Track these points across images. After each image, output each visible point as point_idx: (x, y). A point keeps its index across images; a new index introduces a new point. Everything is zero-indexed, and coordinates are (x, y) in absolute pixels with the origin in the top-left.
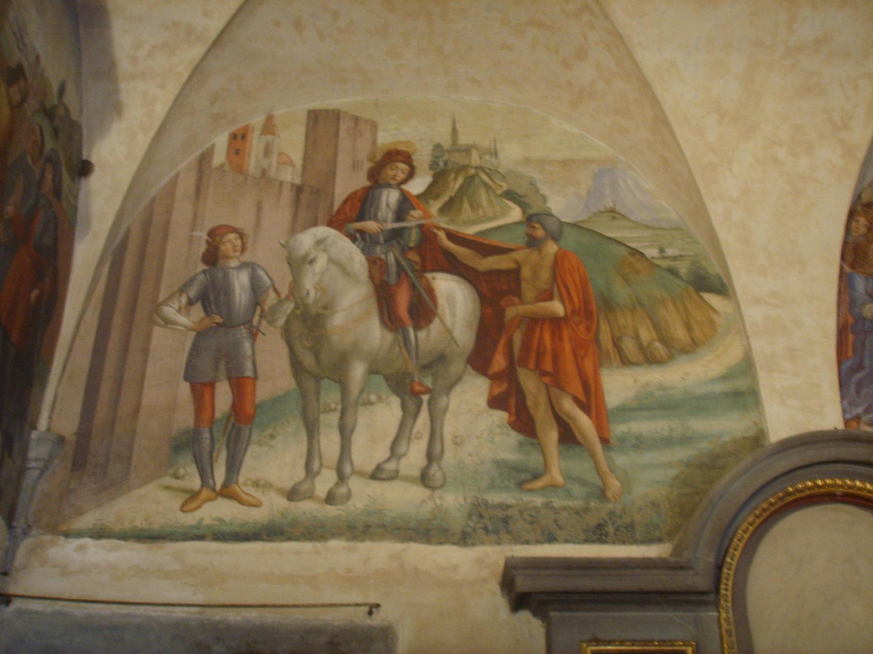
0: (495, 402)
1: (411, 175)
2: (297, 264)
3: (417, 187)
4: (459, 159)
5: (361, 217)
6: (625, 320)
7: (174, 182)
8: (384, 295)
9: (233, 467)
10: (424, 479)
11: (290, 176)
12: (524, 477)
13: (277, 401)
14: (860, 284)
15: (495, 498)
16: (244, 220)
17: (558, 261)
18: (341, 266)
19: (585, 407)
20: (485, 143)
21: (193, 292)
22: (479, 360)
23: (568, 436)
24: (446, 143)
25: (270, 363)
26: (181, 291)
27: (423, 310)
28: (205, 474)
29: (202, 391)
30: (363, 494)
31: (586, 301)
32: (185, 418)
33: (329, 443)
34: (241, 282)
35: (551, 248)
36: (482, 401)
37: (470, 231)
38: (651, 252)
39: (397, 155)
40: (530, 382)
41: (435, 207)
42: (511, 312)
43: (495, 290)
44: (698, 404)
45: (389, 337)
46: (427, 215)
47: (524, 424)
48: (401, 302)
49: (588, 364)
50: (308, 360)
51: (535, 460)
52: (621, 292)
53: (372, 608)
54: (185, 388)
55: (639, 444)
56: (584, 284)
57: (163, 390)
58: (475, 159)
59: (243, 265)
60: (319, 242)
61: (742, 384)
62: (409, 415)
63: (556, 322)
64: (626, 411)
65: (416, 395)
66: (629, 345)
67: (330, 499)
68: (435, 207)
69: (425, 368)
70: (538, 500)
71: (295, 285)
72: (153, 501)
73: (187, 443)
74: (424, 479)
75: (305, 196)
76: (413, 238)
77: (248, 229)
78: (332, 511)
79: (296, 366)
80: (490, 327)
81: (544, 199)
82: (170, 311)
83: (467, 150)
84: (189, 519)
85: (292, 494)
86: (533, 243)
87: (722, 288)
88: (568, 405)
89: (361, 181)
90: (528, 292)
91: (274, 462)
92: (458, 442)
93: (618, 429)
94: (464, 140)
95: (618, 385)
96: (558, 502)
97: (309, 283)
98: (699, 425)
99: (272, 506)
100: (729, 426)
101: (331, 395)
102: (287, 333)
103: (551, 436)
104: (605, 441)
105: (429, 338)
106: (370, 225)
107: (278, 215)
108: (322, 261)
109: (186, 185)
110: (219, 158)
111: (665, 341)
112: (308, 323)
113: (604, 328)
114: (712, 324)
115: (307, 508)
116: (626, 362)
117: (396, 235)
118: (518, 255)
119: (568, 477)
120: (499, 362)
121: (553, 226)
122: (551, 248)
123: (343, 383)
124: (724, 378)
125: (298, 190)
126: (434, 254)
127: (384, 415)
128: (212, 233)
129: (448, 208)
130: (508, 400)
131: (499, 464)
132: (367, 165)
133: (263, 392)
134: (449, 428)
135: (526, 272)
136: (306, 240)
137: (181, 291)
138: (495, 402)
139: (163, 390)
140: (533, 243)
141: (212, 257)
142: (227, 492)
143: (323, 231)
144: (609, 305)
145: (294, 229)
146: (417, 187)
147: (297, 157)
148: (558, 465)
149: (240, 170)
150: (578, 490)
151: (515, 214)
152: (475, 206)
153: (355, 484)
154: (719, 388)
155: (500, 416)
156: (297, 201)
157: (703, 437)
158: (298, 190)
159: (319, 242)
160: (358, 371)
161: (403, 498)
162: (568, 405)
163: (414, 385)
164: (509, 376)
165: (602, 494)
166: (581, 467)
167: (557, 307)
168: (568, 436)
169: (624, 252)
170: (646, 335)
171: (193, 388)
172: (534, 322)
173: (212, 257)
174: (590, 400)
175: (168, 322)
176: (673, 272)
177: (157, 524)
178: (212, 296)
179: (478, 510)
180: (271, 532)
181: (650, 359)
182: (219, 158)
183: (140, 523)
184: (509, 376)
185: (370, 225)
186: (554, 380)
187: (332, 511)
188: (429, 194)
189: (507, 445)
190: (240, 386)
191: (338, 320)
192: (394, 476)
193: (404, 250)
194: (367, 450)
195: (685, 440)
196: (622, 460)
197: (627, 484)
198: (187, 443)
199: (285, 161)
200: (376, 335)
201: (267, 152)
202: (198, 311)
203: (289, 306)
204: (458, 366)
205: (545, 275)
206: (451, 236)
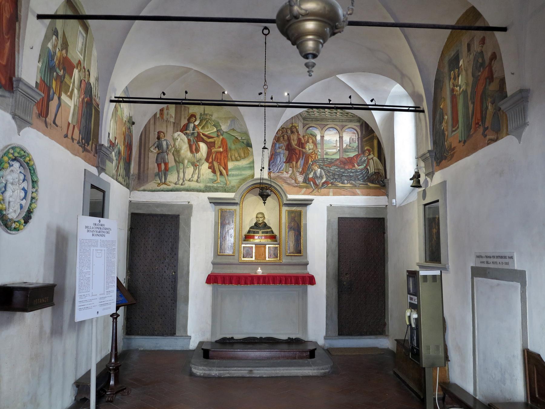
0: (209, 168)
1: (196, 120)
2: (175, 140)
3: (197, 123)
4: (205, 117)
5: (186, 130)
6: (233, 152)
7: (150, 120)
8: (190, 146)
9: (165, 179)
10: (197, 181)
11: (172, 120)
12: (214, 181)
13: (172, 167)
14: (277, 145)
15: (209, 185)
16: (164, 130)
17: (223, 139)
18: (182, 140)
19: (224, 169)
20: (210, 113)
21: (156, 145)
22: (207, 160)
23: (221, 174)
24: (203, 113)
25: (171, 159)
26: (154, 145)
27: (197, 150)
28: (161, 180)
29: (159, 165)
30: (187, 184)
31: (227, 148)
32: (156, 170)
33: (181, 175)
34: (164, 143)
35: (221, 137)
36: (207, 168)
37: (206, 133)
38: (240, 138)
39: (193, 115)
40: (215, 164)
41: (200, 128)
42: (213, 150)
43: (210, 146)
44: (244, 168)
45: (191, 155)
46: (198, 130)
47: (214, 172)
48: (194, 149)
49: (226, 161)
50: (177, 159)
51: (215, 178)
52: (233, 147)
53: (189, 202)
54: (156, 164)
55: (233, 175)
56: (227, 144)
57: (152, 165)
58: (208, 117)
59: (165, 140)
60: (179, 135)
61: (252, 165)
62: (195, 170)
63: (221, 153)
64: (232, 169)
65: (196, 166)
66: (233, 157)
67: (182, 185)
68: (200, 128)
69: (198, 161)
70: (215, 185)
71: (174, 144)
72: (152, 185)
73: (157, 175)
74: (197, 181)
75: (175, 125)
76: (196, 135)
77: (165, 132)
78: (182, 187)
79: (175, 160)
80: (209, 153)
81: (221, 126)
82: (152, 149)
83: (207, 115)
84: (159, 188)
85: (176, 184)
86: (218, 136)
87: (251, 147)
88: (222, 168)
89: (186, 122)
90: (216, 146)
91: (172, 178)
92: (203, 175)
93: (230, 173)
94: (206, 113)
95: (230, 165)
96: (219, 185)
97: (177, 144)
98: (243, 172)
99: (172, 186)
100: (248, 173)
101: (181, 166)
102: (173, 154)
103: (218, 174)
104: (227, 175)
105: (198, 155)
106: (188, 132)
107: (171, 129)
108: (179, 140)
109: (152, 122)
110: (158, 115)
111: (239, 157)
112: (177, 152)
113: (229, 154)
114: (248, 153)
115: (178, 186)
116: (232, 161)
117: (193, 134)
118: (215, 139)
119: (221, 181)
120: (210, 160)
121: (222, 132)
122: (221, 137)
123: (183, 163)
124: (249, 164)
125: (174, 123)
126: (200, 138)
127: (190, 170)
128: (158, 133)
129: (203, 128)
130: (212, 167)
131: (209, 179)
132: (187, 118)
133: (170, 165)
134: (202, 172)
135: (216, 142)
136: (176, 135)
137: (154, 145)
138: (209, 168)
139: (152, 165)
140: (218, 136)
141: (159, 138)
142: (165, 183)
143: (179, 133)
144: (231, 149)
145: (174, 132)
146: (197, 123)
147: (174, 116)
148: (220, 179)
149: (162, 118)
150: (222, 183)
151: (215, 130)
152: (208, 128)
153: (186, 182)
154: (248, 166)
155: (210, 170)
156: (174, 126)
157: (244, 175)
158: (174, 123)
159: (179, 135)
160: (186, 162)
161: (193, 185)
162: (222, 168)
163: (195, 165)
164: (212, 163)
165: (226, 184)
166: (223, 179)
167: (221, 150)
168: (221, 174)
169: (234, 138)
170: (236, 155)
171: (158, 164)
172: (217, 152)
173: (159, 138)
174: (226, 168)
175: (152, 152)
176: (243, 142)
177: (153, 189)
178: (159, 146)
179: (206, 187)
180: (172, 190)
181: (237, 160)
182: (158, 115)
183: (151, 189)
184: (212, 163)
185: (188, 132)
186: (220, 164)
187: (182, 187)
188: (199, 125)
189: (211, 175)
190: (166, 164)
191: (182, 152)
192: (192, 181)
193: (195, 137)
194: (188, 177)
195: (241, 175)
196: (230, 178)
197: (230, 183)
198: (157, 175)
199: (171, 117)
200: (189, 154)
201: (168, 114)
202: (157, 149)
203: (174, 149)
204: (203, 161)
205: (220, 143)
206: (203, 134)
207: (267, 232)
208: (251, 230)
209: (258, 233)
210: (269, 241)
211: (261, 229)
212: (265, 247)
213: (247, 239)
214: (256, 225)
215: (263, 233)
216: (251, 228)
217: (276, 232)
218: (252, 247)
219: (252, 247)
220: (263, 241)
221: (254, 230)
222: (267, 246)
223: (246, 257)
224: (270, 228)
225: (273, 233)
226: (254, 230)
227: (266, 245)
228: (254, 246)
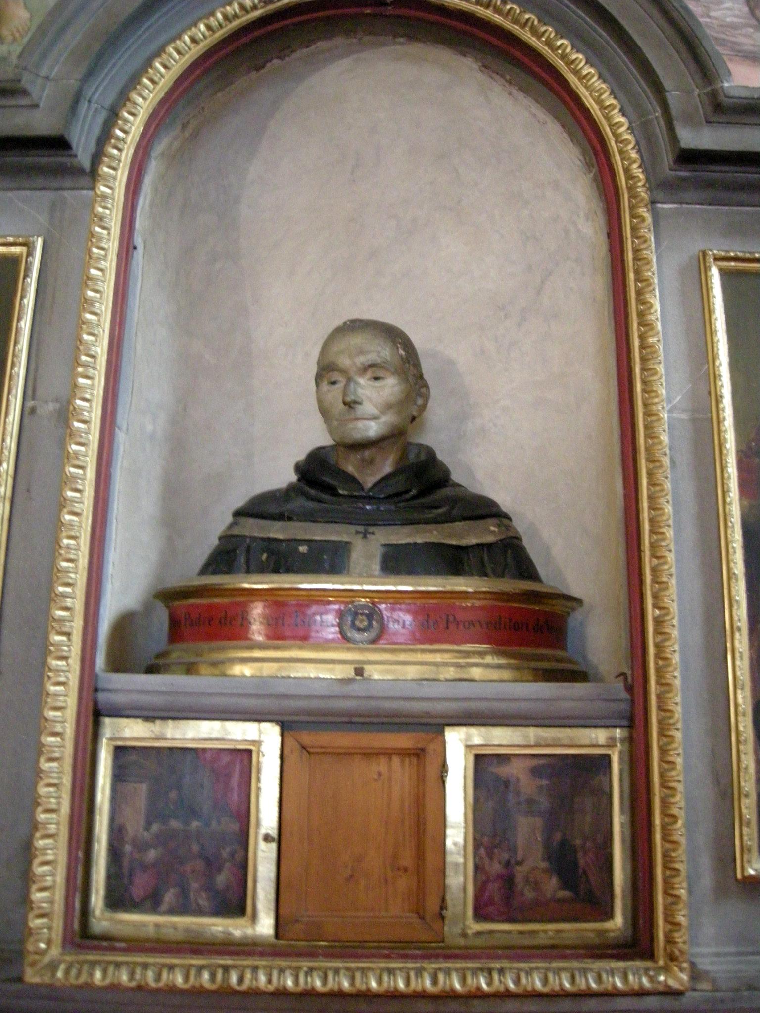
207: (453, 560)
208: (253, 528)
209: (329, 559)
210: (483, 671)
211: (369, 523)
212: (427, 764)
213: (179, 653)
214: (318, 476)
215: (396, 561)
216: (259, 508)
217: (570, 554)
218: (244, 757)
219: (244, 757)
220: (401, 670)
221: (277, 531)
222: (457, 745)
223: (152, 902)
224: (484, 510)
225: (525, 569)
226: (277, 531)
227: (434, 726)
228: (267, 738)
